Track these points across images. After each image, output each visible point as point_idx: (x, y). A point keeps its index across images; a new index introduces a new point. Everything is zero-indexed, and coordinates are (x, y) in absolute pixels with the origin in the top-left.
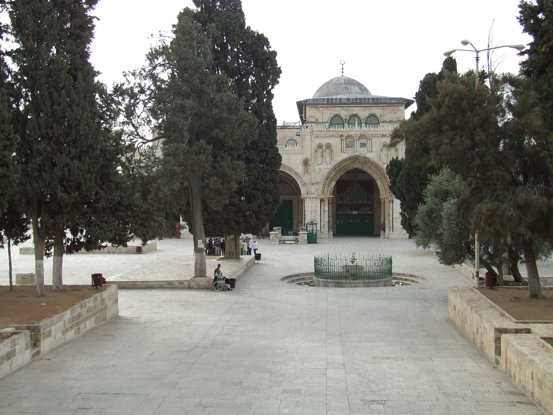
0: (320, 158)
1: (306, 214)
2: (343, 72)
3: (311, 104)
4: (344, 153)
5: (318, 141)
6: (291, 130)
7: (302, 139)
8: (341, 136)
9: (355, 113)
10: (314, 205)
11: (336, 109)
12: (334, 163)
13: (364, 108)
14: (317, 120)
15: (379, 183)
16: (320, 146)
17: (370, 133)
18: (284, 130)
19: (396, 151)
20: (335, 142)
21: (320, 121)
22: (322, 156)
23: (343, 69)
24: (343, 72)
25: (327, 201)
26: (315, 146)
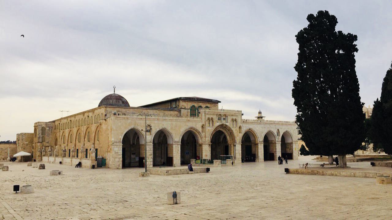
0: (208, 125)
1: (203, 152)
2: (114, 92)
3: (182, 100)
4: (218, 122)
5: (207, 116)
6: (174, 112)
7: (202, 115)
8: (217, 114)
9: (200, 105)
10: (206, 147)
11: (193, 103)
12: (214, 128)
13: (203, 103)
14: (185, 107)
15: (228, 137)
16: (209, 119)
17: (227, 114)
18: (171, 111)
19: (236, 121)
20: (215, 118)
21: (187, 108)
22: (209, 124)
23: (114, 90)
24: (114, 92)
25: (210, 145)
26: (206, 119)
